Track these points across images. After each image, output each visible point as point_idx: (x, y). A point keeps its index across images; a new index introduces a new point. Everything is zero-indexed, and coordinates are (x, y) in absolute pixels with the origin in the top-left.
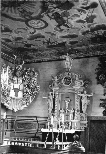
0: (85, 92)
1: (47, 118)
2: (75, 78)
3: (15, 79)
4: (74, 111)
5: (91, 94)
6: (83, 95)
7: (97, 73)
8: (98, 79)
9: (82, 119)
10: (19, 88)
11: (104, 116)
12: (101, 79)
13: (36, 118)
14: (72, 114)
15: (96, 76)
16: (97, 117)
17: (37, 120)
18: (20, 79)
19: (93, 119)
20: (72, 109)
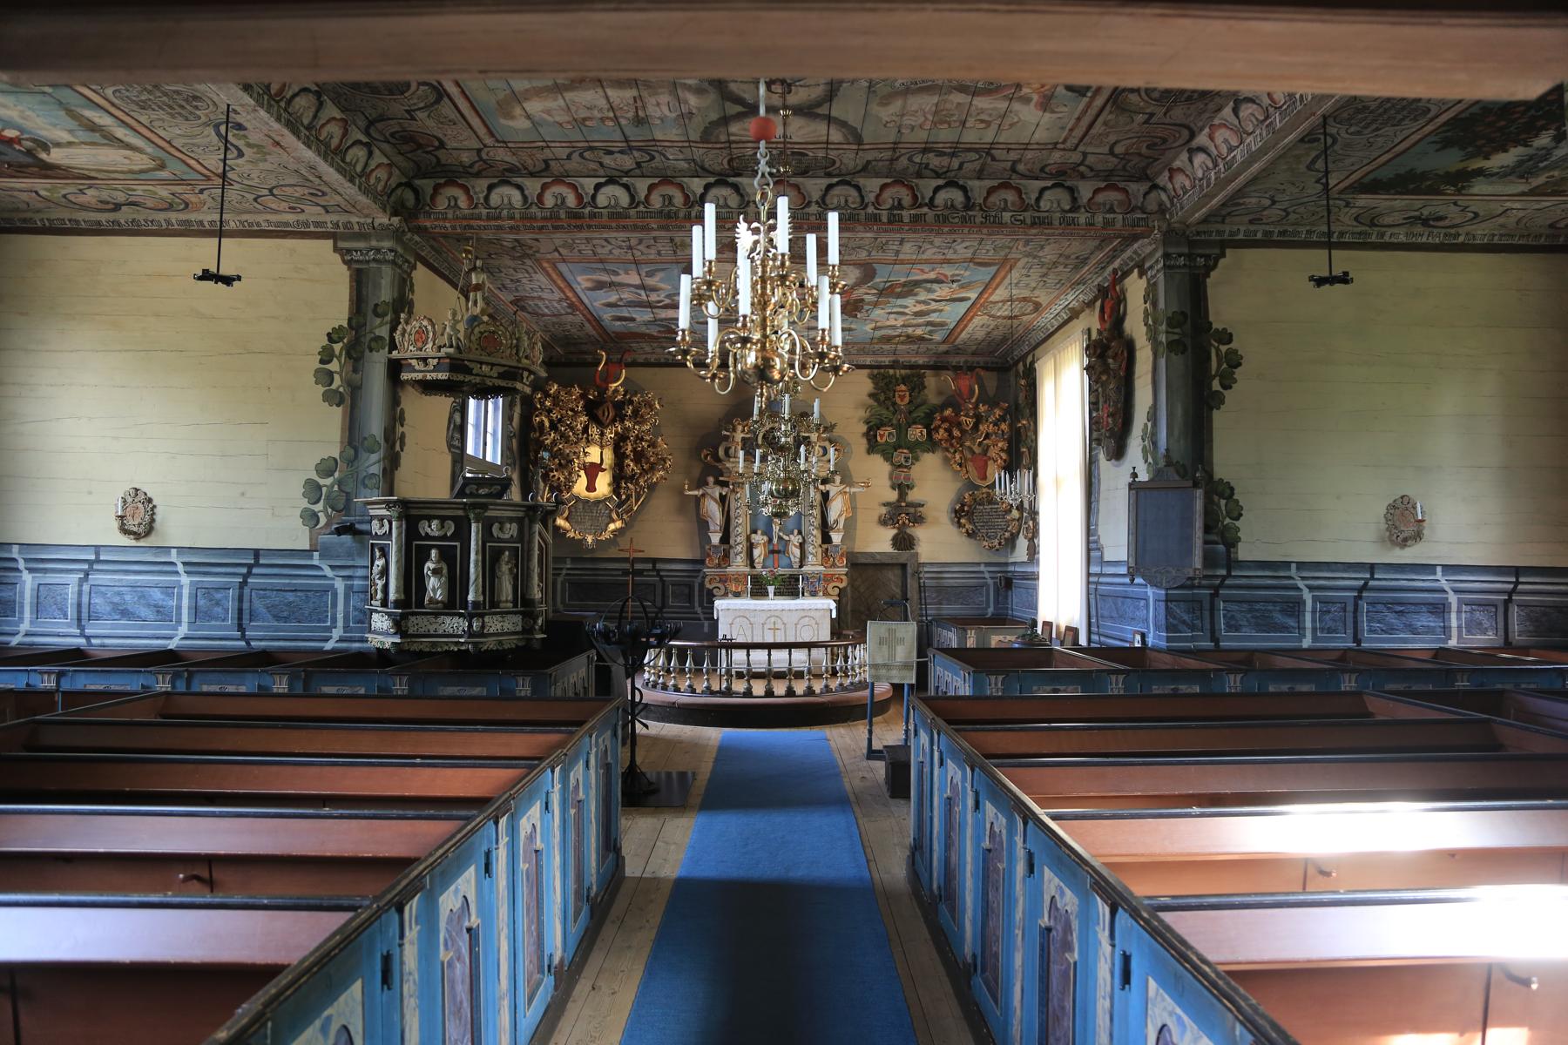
0: (838, 479)
2: (806, 435)
6: (833, 489)
7: (867, 422)
10: (598, 461)
13: (654, 566)
14: (795, 546)
15: (864, 428)
16: (872, 555)
17: (659, 571)
18: (610, 435)
19: (863, 561)
20: (796, 532)
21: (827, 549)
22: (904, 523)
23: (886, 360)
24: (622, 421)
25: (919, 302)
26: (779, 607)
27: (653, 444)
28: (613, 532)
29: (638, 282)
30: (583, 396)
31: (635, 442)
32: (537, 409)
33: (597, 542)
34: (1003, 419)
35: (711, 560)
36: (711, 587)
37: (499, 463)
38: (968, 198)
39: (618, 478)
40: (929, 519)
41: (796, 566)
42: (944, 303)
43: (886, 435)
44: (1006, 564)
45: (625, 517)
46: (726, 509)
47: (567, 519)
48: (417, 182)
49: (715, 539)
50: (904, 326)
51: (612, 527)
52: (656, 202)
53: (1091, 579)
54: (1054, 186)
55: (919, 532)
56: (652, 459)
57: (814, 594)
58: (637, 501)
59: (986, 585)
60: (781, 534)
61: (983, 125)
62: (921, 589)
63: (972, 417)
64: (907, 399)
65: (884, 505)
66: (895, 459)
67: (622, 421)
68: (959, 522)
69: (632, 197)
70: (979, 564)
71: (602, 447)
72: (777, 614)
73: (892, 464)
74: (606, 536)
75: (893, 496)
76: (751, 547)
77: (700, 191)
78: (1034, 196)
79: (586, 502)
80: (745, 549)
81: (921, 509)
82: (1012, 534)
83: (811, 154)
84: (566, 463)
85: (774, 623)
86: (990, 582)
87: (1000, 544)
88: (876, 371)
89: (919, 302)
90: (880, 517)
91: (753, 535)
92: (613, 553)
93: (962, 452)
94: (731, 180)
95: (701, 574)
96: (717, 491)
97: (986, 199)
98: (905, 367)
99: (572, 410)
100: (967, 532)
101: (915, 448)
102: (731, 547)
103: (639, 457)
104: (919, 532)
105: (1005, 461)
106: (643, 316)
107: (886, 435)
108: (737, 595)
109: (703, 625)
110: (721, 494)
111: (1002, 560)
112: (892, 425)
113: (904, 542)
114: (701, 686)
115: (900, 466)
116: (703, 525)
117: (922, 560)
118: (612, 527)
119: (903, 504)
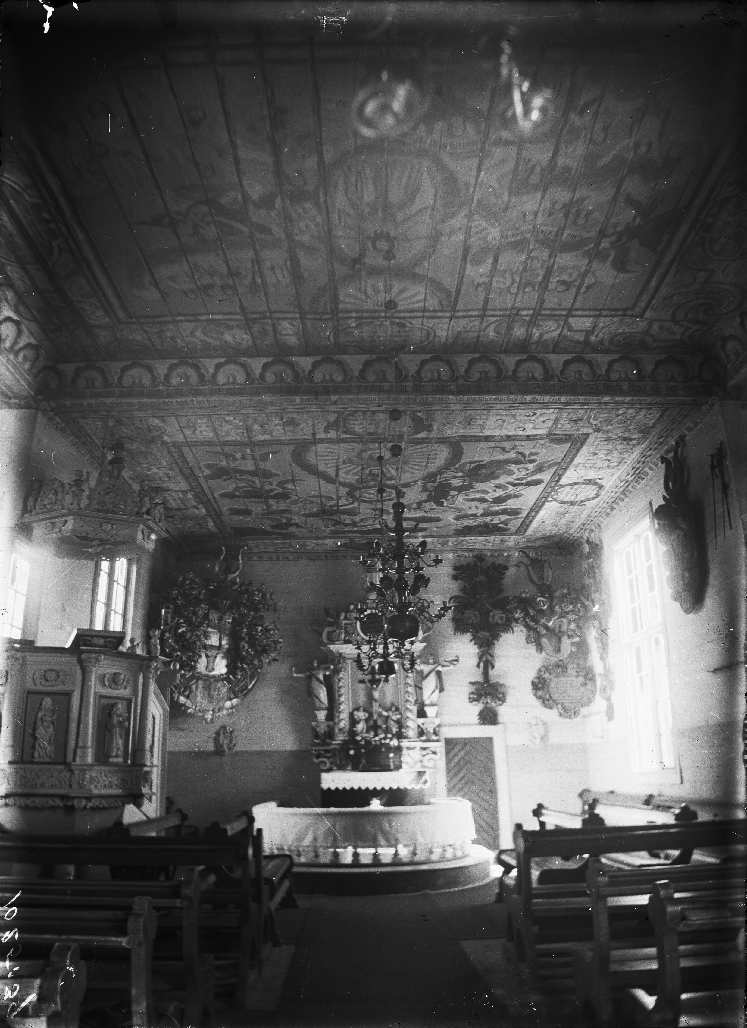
3: (214, 616)
25: (498, 487)
29: (252, 468)
38: (546, 370)
42: (520, 487)
48: (62, 367)
52: (270, 377)
54: (620, 359)
61: (562, 288)
69: (248, 375)
77: (308, 368)
78: (604, 368)
83: (409, 325)
89: (498, 487)
94: (336, 357)
97: (562, 371)
103: (252, 640)
106: (258, 507)
110: (325, 676)
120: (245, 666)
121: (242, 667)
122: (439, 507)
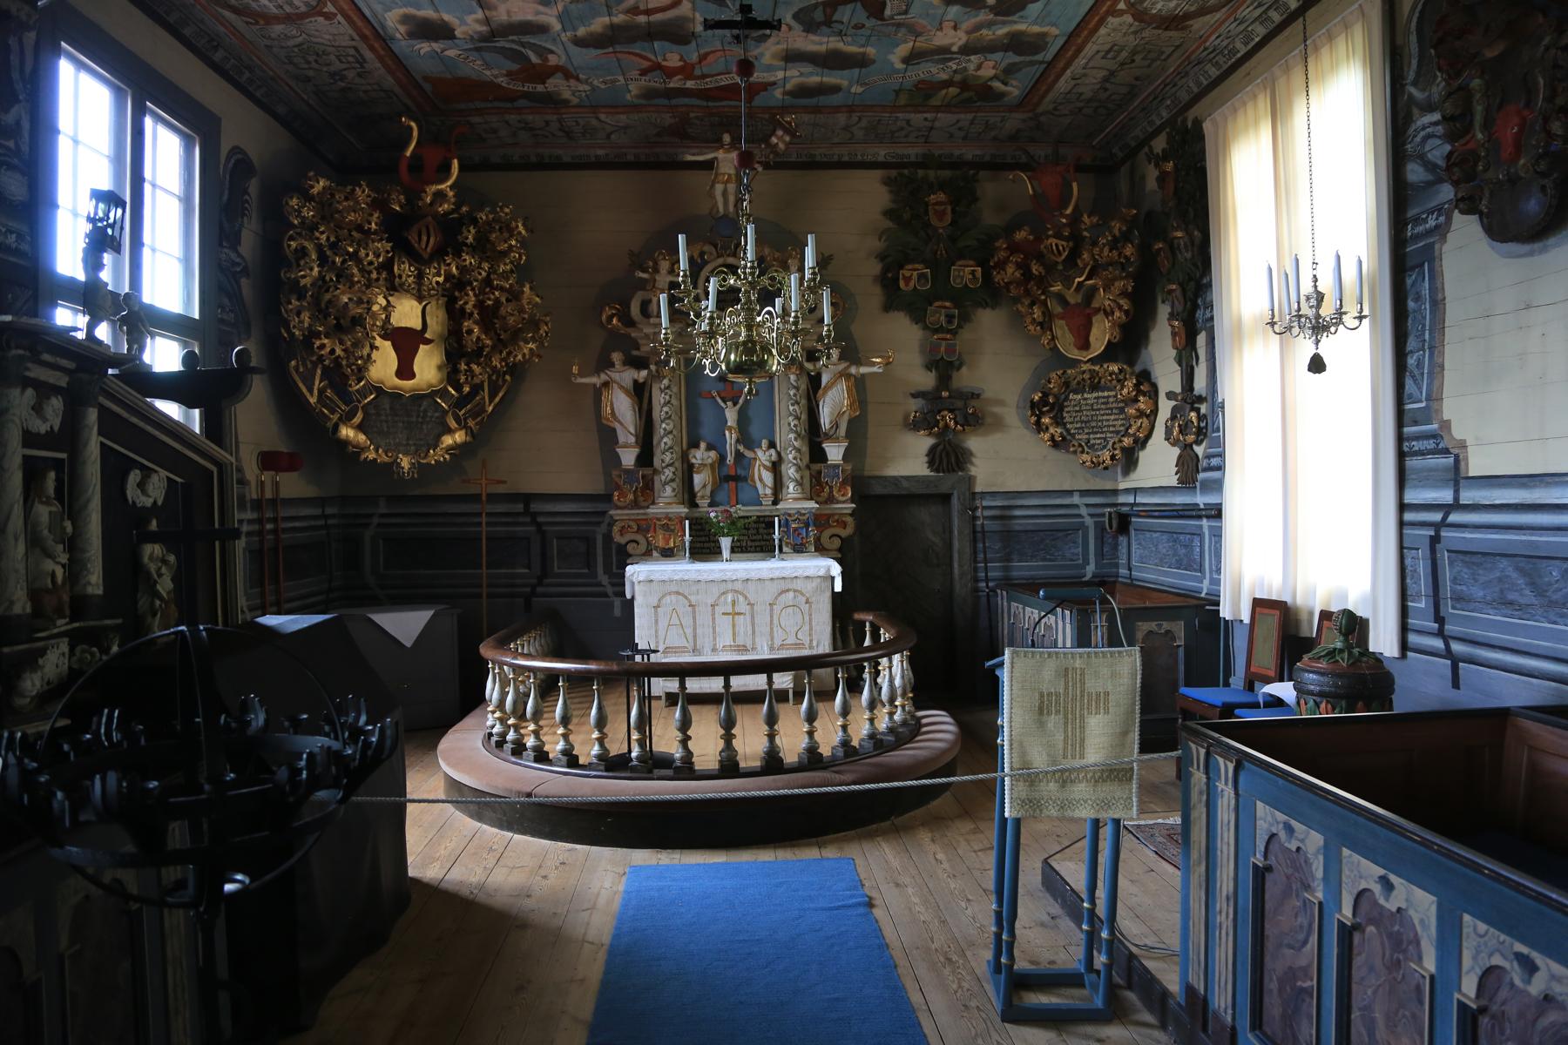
1: (607, 498)
4: (773, 451)
5: (874, 364)
7: (882, 257)
8: (888, 282)
9: (825, 494)
11: (932, 474)
12: (907, 285)
13: (527, 506)
14: (765, 467)
15: (875, 268)
16: (896, 480)
17: (534, 515)
19: (878, 490)
20: (765, 443)
21: (820, 473)
22: (947, 426)
23: (913, 152)
24: (457, 254)
26: (742, 575)
27: (514, 296)
28: (449, 449)
30: (376, 204)
31: (482, 292)
32: (293, 226)
33: (423, 469)
34: (1126, 237)
35: (622, 495)
36: (623, 541)
37: (197, 316)
39: (455, 353)
40: (989, 420)
41: (768, 501)
43: (912, 277)
44: (1115, 492)
45: (471, 423)
46: (646, 401)
47: (360, 428)
49: (628, 457)
50: (967, 50)
51: (448, 440)
53: (1408, 516)
55: (974, 443)
56: (511, 320)
57: (799, 549)
58: (492, 397)
59: (1083, 526)
60: (741, 448)
62: (976, 535)
63: (1067, 239)
64: (949, 218)
65: (914, 396)
66: (930, 319)
67: (457, 254)
68: (1038, 423)
70: (1070, 493)
71: (420, 299)
72: (738, 586)
73: (926, 328)
74: (435, 456)
75: (927, 380)
76: (688, 470)
79: (396, 396)
80: (679, 474)
81: (974, 403)
82: (1136, 442)
84: (350, 325)
85: (734, 603)
86: (1089, 521)
87: (1113, 458)
88: (894, 173)
90: (906, 417)
91: (693, 451)
92: (455, 487)
93: (1045, 303)
95: (607, 520)
96: (628, 376)
98: (942, 166)
99: (360, 228)
100: (1052, 438)
101: (966, 303)
102: (656, 472)
103: (488, 316)
104: (974, 443)
105: (1127, 312)
107: (912, 277)
108: (668, 554)
109: (611, 605)
111: (1109, 486)
112: (923, 262)
113: (949, 457)
114: (589, 751)
115: (936, 331)
116: (608, 437)
117: (978, 489)
118: (448, 440)
119: (945, 394)
120: (474, 367)
121: (470, 370)
122: (872, 22)
